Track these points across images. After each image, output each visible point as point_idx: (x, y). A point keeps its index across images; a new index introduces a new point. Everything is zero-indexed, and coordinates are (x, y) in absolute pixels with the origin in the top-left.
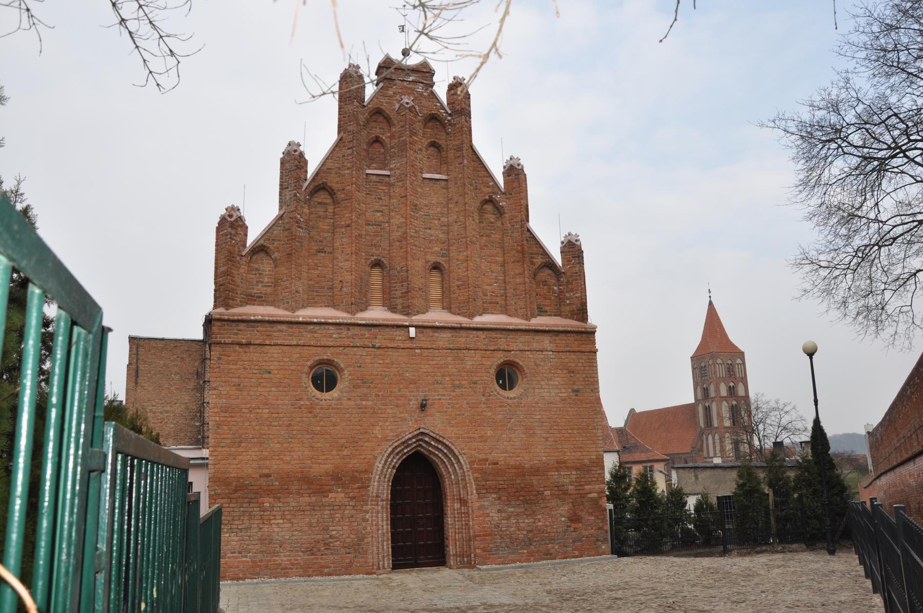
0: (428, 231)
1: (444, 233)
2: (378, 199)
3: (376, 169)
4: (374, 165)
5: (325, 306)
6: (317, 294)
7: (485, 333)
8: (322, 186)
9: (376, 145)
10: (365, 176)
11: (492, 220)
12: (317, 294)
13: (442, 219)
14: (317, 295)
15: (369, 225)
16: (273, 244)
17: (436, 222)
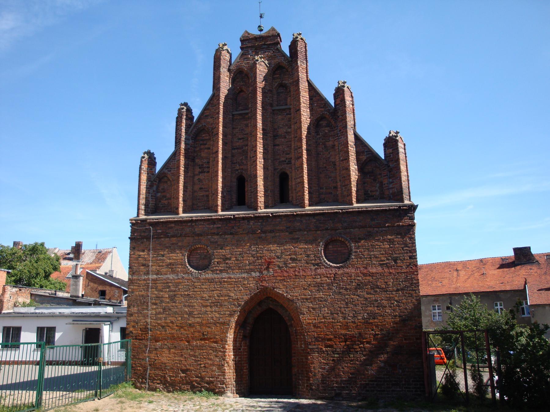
0: (277, 147)
1: (288, 147)
2: (242, 130)
3: (242, 110)
4: (240, 108)
5: (205, 209)
6: (198, 201)
7: (316, 217)
8: (202, 128)
9: (242, 94)
10: (231, 117)
11: (326, 131)
12: (198, 201)
13: (287, 137)
14: (199, 202)
15: (235, 149)
16: (170, 171)
17: (283, 140)
